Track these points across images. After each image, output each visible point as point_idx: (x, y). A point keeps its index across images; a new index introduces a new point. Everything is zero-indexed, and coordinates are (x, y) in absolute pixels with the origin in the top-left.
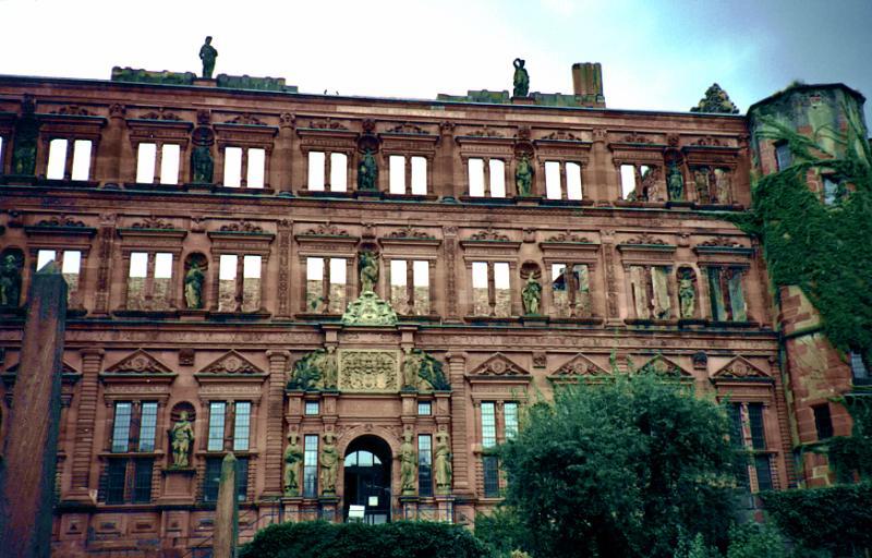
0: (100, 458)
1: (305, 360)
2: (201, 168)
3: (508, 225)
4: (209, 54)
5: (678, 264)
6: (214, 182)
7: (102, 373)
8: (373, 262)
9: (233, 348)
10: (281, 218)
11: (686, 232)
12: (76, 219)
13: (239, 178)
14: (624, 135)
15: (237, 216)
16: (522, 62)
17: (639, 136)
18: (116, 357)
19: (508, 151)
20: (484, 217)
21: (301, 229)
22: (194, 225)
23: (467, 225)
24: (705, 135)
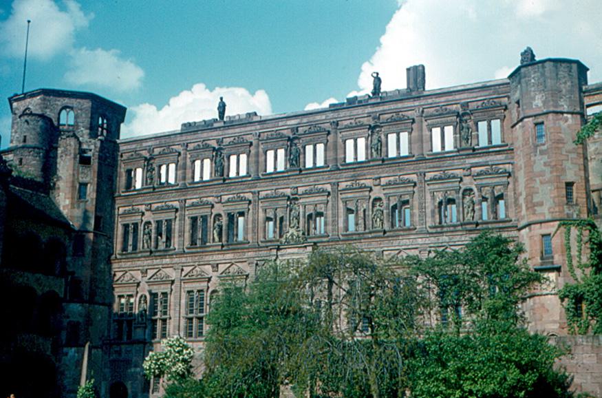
0: (183, 317)
1: (263, 265)
2: (220, 170)
3: (364, 177)
4: (222, 108)
5: (463, 187)
6: (225, 176)
7: (182, 278)
8: (297, 208)
9: (233, 261)
10: (253, 190)
11: (468, 166)
12: (170, 203)
13: (235, 171)
14: (433, 109)
15: (234, 192)
16: (378, 74)
17: (443, 107)
18: (187, 269)
19: (367, 132)
20: (352, 173)
21: (263, 194)
22: (216, 200)
23: (344, 180)
24: (485, 99)
